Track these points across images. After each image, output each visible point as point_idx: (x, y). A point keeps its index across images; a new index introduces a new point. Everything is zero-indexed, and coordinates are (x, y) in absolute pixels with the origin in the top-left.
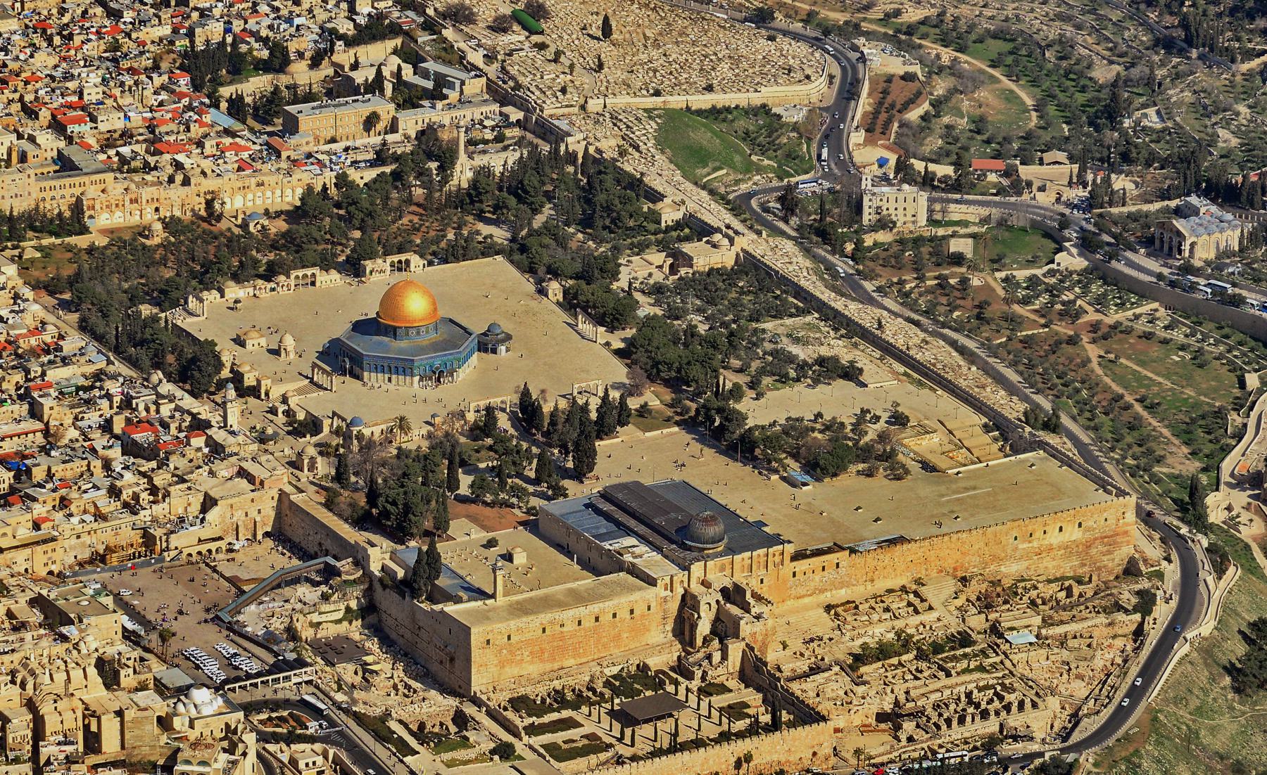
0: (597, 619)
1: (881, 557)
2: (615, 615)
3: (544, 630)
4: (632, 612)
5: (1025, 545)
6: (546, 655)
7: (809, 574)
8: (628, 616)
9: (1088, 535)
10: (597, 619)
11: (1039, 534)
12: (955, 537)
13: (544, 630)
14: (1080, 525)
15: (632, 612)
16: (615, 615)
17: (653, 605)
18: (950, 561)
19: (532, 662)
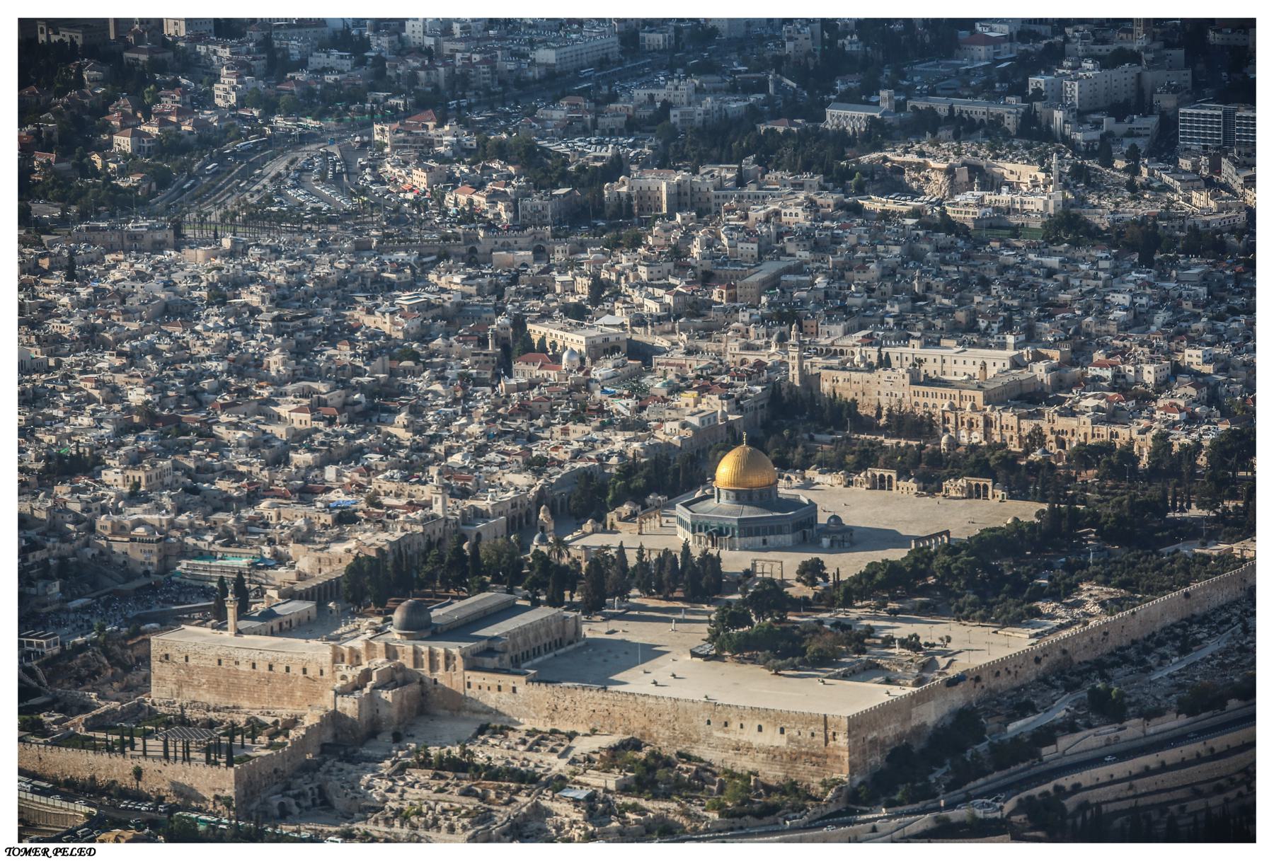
0: (271, 667)
2: (288, 669)
3: (220, 662)
4: (305, 671)
6: (222, 688)
7: (485, 689)
8: (301, 675)
9: (793, 746)
10: (271, 667)
11: (735, 725)
12: (640, 699)
13: (220, 662)
14: (782, 731)
15: (305, 671)
16: (288, 669)
17: (326, 670)
18: (636, 725)
19: (208, 692)
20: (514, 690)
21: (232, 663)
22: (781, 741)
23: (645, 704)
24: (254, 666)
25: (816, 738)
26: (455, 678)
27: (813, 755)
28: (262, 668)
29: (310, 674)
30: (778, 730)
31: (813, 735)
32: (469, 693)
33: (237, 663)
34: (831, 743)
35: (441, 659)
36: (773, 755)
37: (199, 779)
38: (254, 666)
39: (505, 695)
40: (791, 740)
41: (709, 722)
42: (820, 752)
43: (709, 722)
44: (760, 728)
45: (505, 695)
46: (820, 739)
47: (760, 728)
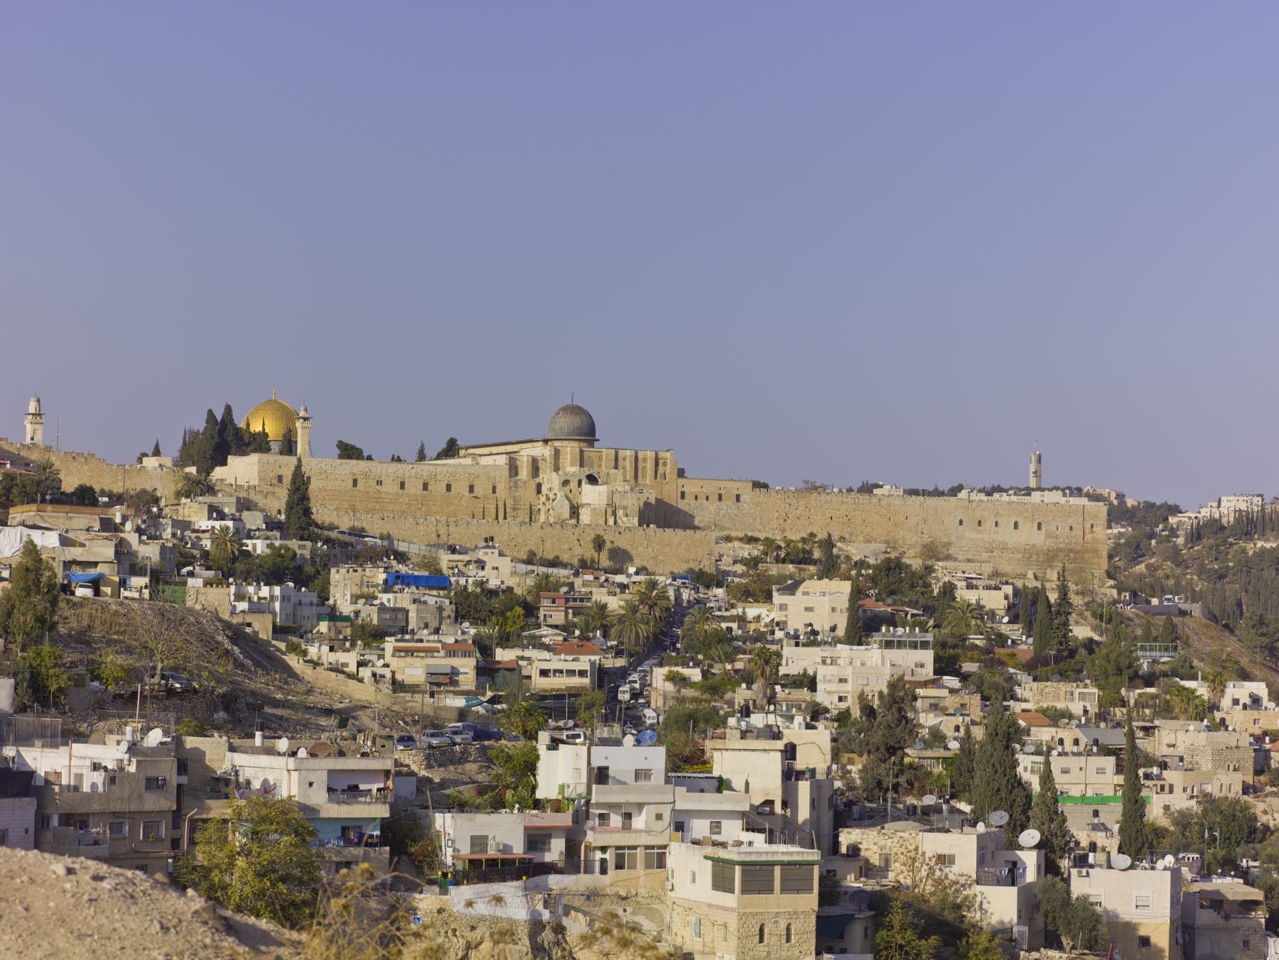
0: (425, 487)
1: (793, 502)
2: (449, 487)
3: (355, 482)
4: (471, 489)
5: (974, 535)
7: (702, 500)
8: (467, 494)
9: (1051, 543)
10: (425, 487)
11: (989, 524)
13: (355, 482)
15: (471, 489)
16: (449, 487)
17: (500, 487)
20: (738, 498)
21: (373, 483)
22: (1038, 539)
23: (889, 505)
24: (402, 486)
25: (1074, 532)
26: (666, 488)
27: (1071, 551)
28: (414, 488)
29: (478, 491)
30: (1036, 526)
31: (1071, 528)
32: (682, 505)
33: (379, 483)
34: (1088, 536)
35: (650, 465)
36: (1029, 554)
37: (666, 551)
38: (402, 486)
39: (728, 504)
40: (1048, 536)
41: (961, 522)
42: (1079, 548)
43: (961, 522)
44: (1016, 526)
45: (728, 504)
46: (1078, 532)
47: (1016, 526)
